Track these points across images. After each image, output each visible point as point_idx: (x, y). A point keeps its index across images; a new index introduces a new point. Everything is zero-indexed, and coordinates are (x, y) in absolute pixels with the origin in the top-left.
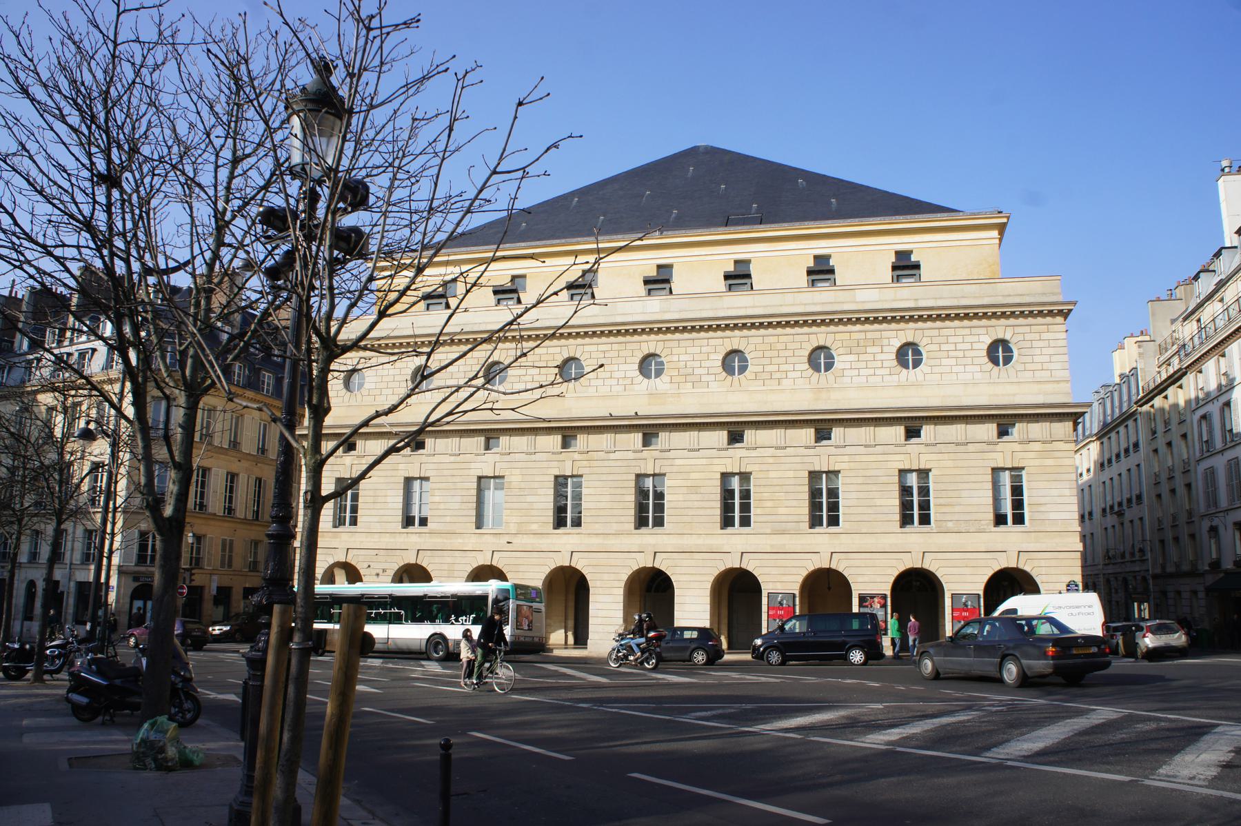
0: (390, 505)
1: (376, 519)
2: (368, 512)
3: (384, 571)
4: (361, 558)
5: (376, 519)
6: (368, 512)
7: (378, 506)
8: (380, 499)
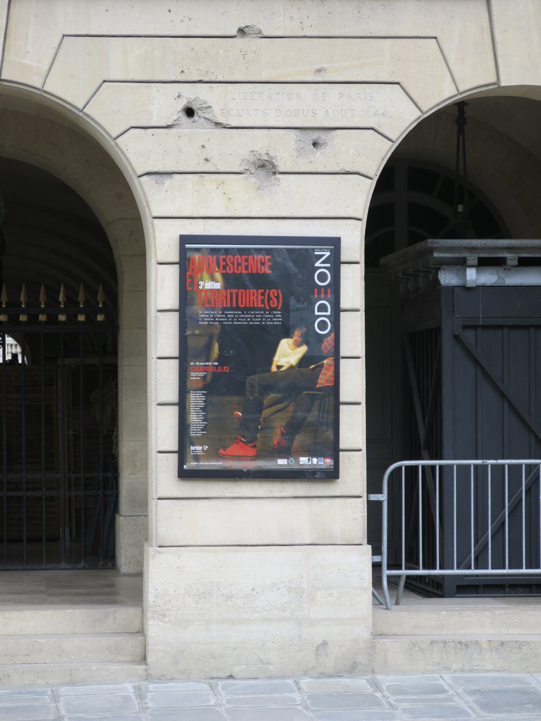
4: (124, 60)
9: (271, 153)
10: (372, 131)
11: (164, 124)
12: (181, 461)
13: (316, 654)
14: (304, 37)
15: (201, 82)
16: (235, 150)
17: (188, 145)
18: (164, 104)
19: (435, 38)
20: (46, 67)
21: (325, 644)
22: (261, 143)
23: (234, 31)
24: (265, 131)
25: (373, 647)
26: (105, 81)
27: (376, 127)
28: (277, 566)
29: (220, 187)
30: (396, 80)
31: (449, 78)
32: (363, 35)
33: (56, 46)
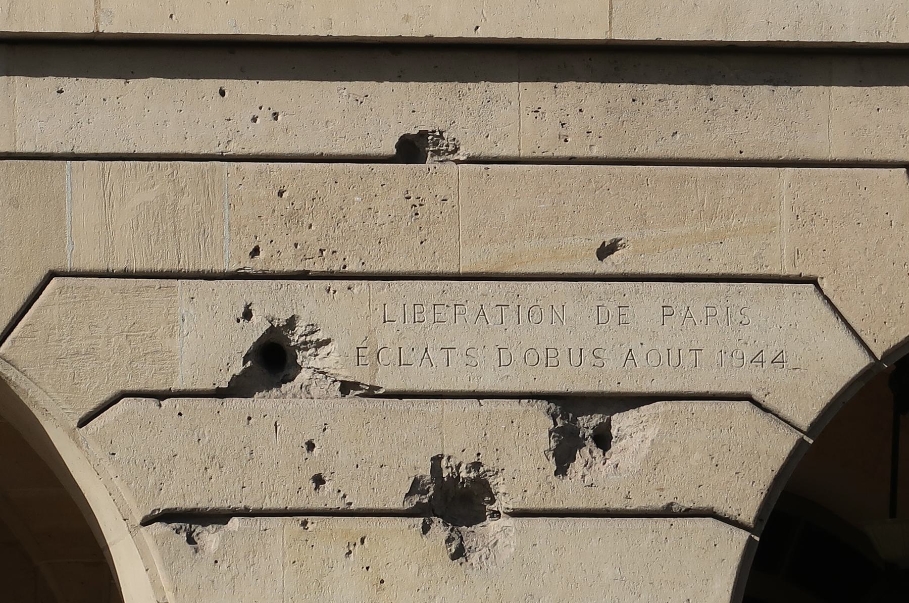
3: (580, 420)
4: (101, 218)
9: (488, 463)
10: (746, 403)
11: (208, 386)
14: (572, 161)
15: (303, 275)
16: (391, 454)
18: (209, 336)
22: (455, 437)
23: (390, 149)
24: (471, 405)
26: (52, 275)
27: (758, 395)
29: (357, 550)
30: (807, 271)
32: (722, 155)
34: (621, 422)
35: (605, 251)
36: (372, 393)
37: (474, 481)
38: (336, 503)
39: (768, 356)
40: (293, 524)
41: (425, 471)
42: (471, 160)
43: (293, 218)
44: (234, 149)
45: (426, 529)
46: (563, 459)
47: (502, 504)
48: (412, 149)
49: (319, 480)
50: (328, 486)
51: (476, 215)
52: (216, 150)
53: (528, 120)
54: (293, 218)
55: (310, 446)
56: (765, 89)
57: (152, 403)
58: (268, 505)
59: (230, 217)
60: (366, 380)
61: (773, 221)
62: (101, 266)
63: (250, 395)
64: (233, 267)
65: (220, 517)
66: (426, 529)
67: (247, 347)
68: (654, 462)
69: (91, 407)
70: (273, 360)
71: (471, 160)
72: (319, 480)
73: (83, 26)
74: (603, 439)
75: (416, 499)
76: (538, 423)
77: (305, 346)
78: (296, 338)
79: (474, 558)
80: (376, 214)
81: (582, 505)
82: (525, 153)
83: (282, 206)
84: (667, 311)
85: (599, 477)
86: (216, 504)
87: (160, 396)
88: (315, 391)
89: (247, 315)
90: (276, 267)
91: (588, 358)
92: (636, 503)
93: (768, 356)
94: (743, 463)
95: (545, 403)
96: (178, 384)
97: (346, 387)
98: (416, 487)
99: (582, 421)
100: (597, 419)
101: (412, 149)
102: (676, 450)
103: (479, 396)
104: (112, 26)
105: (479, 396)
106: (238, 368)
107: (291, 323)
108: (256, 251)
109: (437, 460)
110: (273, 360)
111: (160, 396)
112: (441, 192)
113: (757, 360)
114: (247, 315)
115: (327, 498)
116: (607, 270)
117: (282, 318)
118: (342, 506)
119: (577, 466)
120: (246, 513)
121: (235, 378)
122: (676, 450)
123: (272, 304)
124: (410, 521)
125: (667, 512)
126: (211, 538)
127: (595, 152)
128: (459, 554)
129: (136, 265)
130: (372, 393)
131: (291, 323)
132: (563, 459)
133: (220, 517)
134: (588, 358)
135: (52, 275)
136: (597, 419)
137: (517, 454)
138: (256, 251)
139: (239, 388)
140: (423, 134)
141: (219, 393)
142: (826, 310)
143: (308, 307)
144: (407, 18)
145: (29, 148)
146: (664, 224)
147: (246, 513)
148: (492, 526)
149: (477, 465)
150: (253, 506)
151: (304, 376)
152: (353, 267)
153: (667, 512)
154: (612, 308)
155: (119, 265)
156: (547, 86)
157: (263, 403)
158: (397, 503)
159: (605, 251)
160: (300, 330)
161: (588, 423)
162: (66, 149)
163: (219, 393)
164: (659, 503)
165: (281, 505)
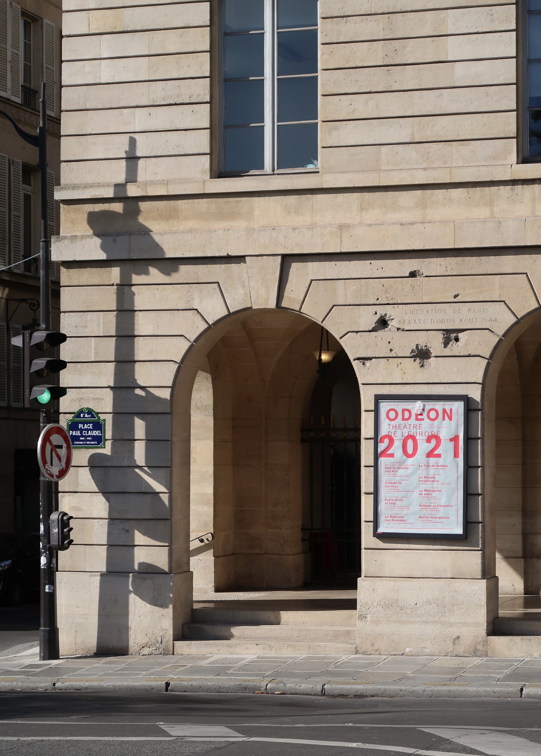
0: (461, 73)
1: (402, 131)
2: (362, 106)
3: (450, 336)
4: (344, 293)
5: (402, 131)
6: (362, 106)
7: (408, 77)
8: (413, 51)
12: (376, 527)
13: (454, 644)
14: (448, 276)
16: (407, 344)
17: (379, 343)
18: (368, 318)
19: (526, 274)
20: (302, 299)
21: (458, 637)
22: (422, 339)
25: (486, 641)
26: (334, 306)
27: (490, 329)
28: (427, 590)
31: (534, 298)
32: (483, 273)
33: (307, 286)
34: (460, 335)
35: (455, 296)
36: (403, 330)
37: (426, 349)
38: (395, 355)
39: (493, 319)
40: (385, 360)
41: (414, 348)
42: (426, 277)
43: (386, 291)
44: (373, 276)
45: (415, 361)
46: (446, 344)
47: (433, 355)
48: (413, 275)
49: (391, 350)
50: (393, 352)
51: (425, 289)
52: (369, 277)
53: (438, 267)
54: (386, 291)
55: (389, 343)
56: (493, 257)
57: (355, 333)
58: (380, 356)
59: (373, 291)
60: (402, 328)
61: (494, 288)
62: (344, 304)
63: (377, 331)
64: (373, 303)
65: (370, 359)
66: (415, 361)
67: (376, 321)
68: (466, 345)
69: (342, 335)
70: (383, 323)
71: (426, 277)
72: (391, 350)
73: (338, 251)
74: (457, 340)
75: (413, 354)
76: (440, 336)
77: (389, 320)
78: (387, 318)
79: (426, 367)
80: (405, 290)
81: (449, 355)
82: (438, 274)
83: (384, 288)
84: (469, 310)
85: (454, 348)
86: (369, 356)
87: (357, 332)
88: (392, 330)
89: (376, 313)
90: (382, 303)
91: (451, 321)
92: (461, 354)
93: (493, 319)
94: (485, 344)
95: (442, 332)
96: (360, 330)
97: (398, 329)
98: (413, 351)
99: (452, 335)
100: (455, 335)
101: (413, 275)
102: (471, 341)
103: (427, 330)
104: (344, 250)
105: (427, 330)
106: (374, 325)
107: (386, 315)
108: (378, 299)
109: (417, 345)
110: (383, 323)
111: (357, 332)
112: (419, 284)
113: (491, 320)
114: (376, 313)
115: (393, 354)
116: (456, 300)
117: (383, 314)
118: (396, 356)
119: (449, 346)
120: (375, 358)
121: (373, 328)
122: (471, 341)
123: (381, 311)
124: (410, 359)
125: (469, 356)
126: (368, 363)
127: (454, 274)
128: (422, 366)
129: (352, 303)
130: (403, 330)
131: (386, 315)
132: (446, 344)
133: (370, 359)
134: (451, 321)
135: (334, 306)
136: (455, 335)
137: (435, 343)
138: (378, 299)
139: (374, 330)
140: (415, 271)
141: (370, 331)
142: (506, 308)
143: (389, 311)
144: (408, 245)
145: (329, 278)
146: (468, 289)
147: (375, 358)
148: (431, 359)
149: (426, 346)
150: (377, 356)
151: (390, 327)
152: (399, 302)
153: (469, 356)
154: (457, 309)
155: (348, 304)
156: (443, 259)
157: (380, 333)
158: (408, 356)
159: (455, 296)
160: (388, 316)
161: (453, 336)
162: (337, 278)
163: (370, 331)
164: (467, 354)
165: (383, 356)
